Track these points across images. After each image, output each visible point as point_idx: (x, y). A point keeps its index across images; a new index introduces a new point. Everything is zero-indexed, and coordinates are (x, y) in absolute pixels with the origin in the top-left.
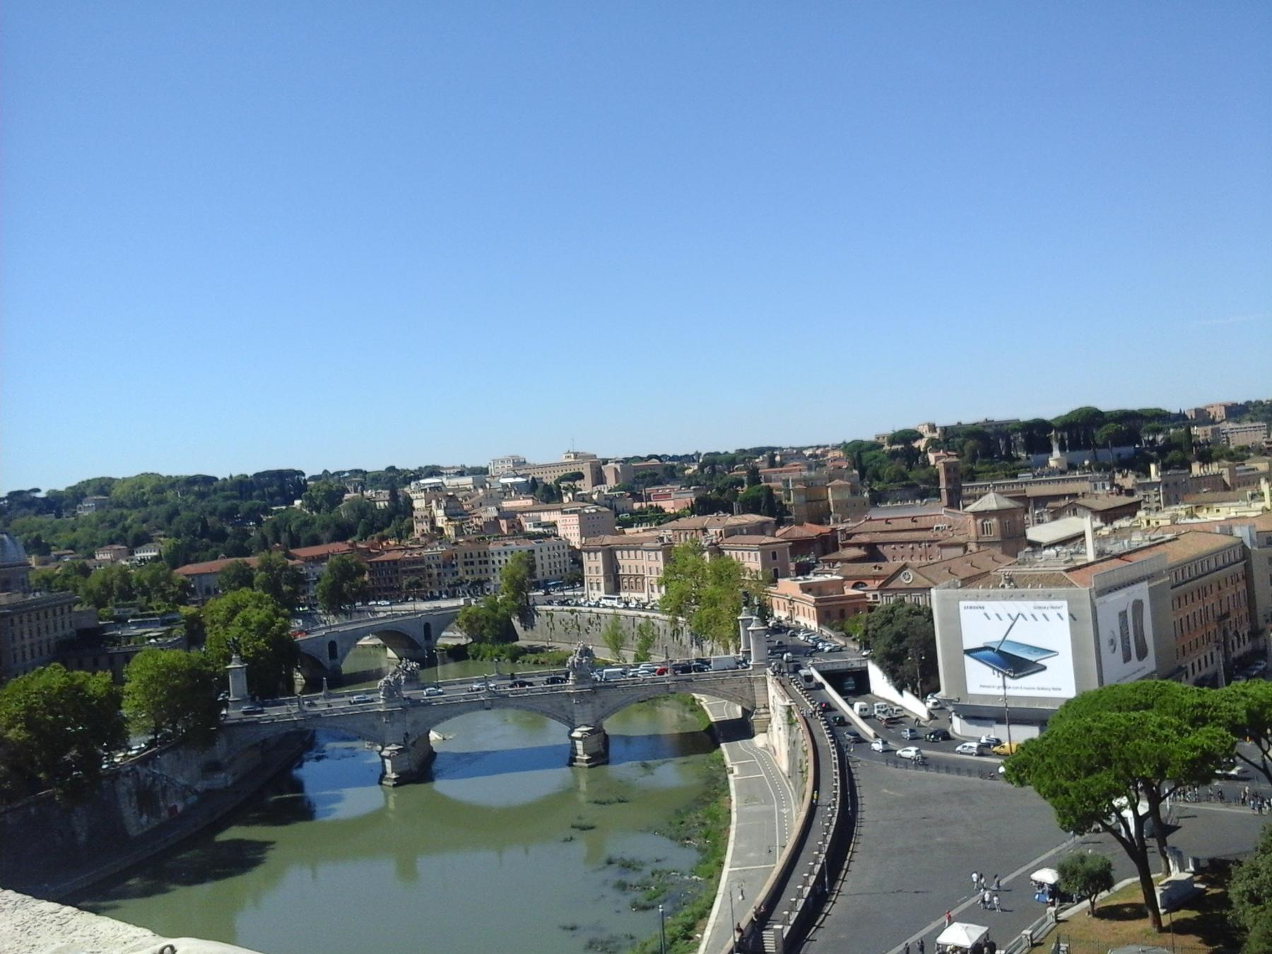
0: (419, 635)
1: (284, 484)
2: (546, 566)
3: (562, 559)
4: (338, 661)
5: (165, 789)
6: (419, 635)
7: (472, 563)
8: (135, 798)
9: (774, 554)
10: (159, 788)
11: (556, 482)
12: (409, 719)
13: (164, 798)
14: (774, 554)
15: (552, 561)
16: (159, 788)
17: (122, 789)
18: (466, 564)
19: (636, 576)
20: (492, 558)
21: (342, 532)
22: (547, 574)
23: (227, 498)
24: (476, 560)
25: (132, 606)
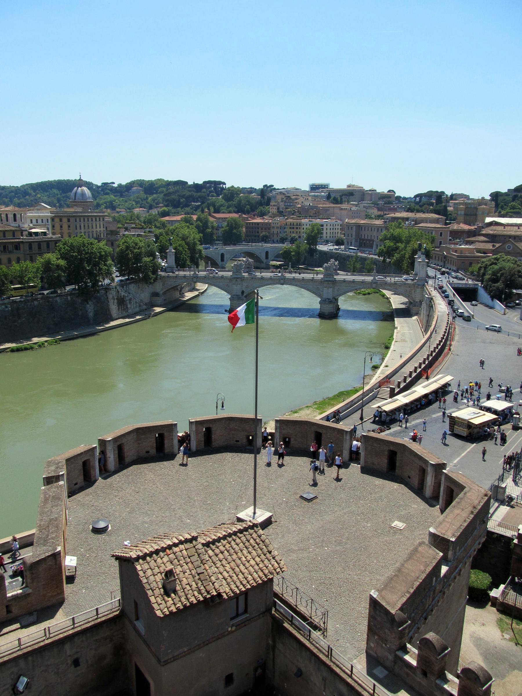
0: (263, 257)
1: (215, 187)
2: (328, 233)
3: (337, 231)
4: (224, 263)
5: (130, 300)
6: (263, 257)
7: (293, 228)
8: (116, 301)
9: (441, 233)
10: (127, 298)
11: (341, 196)
12: (245, 284)
13: (130, 303)
14: (441, 233)
15: (332, 231)
16: (127, 298)
17: (110, 296)
18: (290, 228)
19: (370, 240)
20: (303, 227)
21: (240, 210)
22: (328, 238)
23: (190, 191)
24: (295, 227)
25: (132, 223)
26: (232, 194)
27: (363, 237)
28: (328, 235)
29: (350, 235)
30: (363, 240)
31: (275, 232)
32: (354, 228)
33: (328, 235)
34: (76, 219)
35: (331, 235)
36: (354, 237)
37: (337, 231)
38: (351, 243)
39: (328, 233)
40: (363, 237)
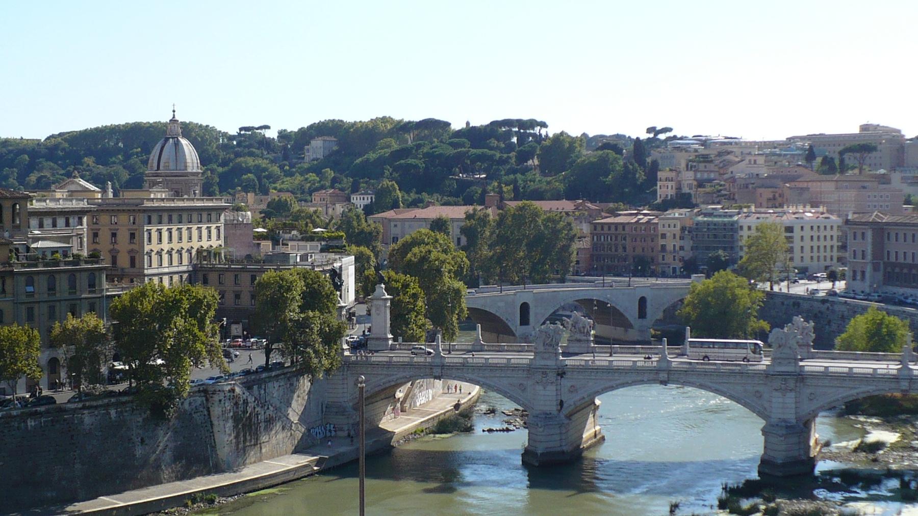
2: (807, 249)
15: (815, 243)
26: (560, 150)
27: (893, 259)
28: (807, 254)
29: (859, 255)
30: (894, 265)
31: (670, 248)
32: (869, 234)
33: (807, 254)
34: (150, 217)
35: (815, 254)
36: (869, 257)
37: (829, 243)
38: (863, 273)
39: (807, 249)
40: (893, 259)
